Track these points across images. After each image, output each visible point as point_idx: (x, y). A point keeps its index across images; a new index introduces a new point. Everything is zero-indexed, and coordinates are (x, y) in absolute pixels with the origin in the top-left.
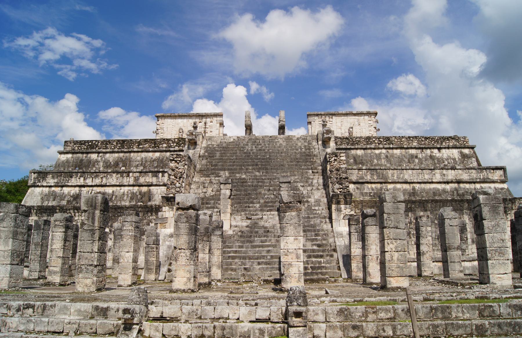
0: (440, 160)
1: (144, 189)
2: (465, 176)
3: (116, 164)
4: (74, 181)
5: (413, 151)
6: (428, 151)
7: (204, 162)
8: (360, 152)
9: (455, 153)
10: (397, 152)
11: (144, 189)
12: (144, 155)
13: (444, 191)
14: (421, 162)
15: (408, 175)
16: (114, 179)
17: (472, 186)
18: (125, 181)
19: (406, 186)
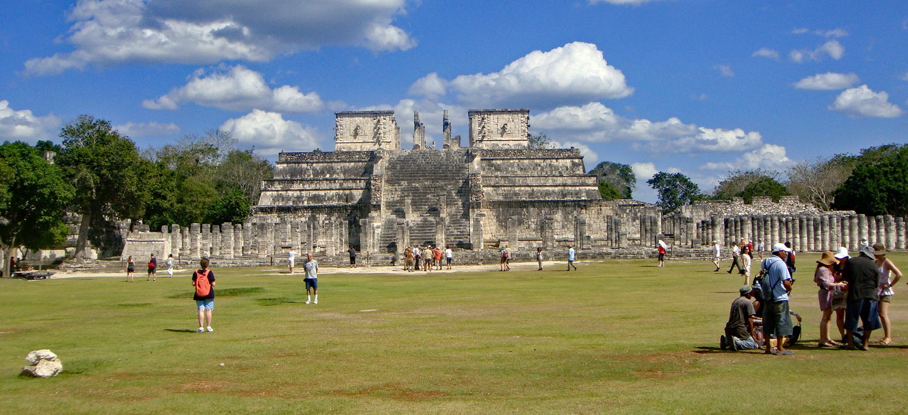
0: (557, 168)
1: (347, 192)
2: (569, 182)
3: (322, 173)
4: (296, 186)
5: (538, 161)
6: (548, 161)
7: (390, 173)
8: (499, 162)
9: (568, 162)
10: (526, 162)
11: (347, 192)
12: (342, 164)
13: (554, 192)
14: (542, 170)
15: (530, 181)
16: (324, 185)
17: (573, 188)
18: (333, 186)
19: (527, 188)
